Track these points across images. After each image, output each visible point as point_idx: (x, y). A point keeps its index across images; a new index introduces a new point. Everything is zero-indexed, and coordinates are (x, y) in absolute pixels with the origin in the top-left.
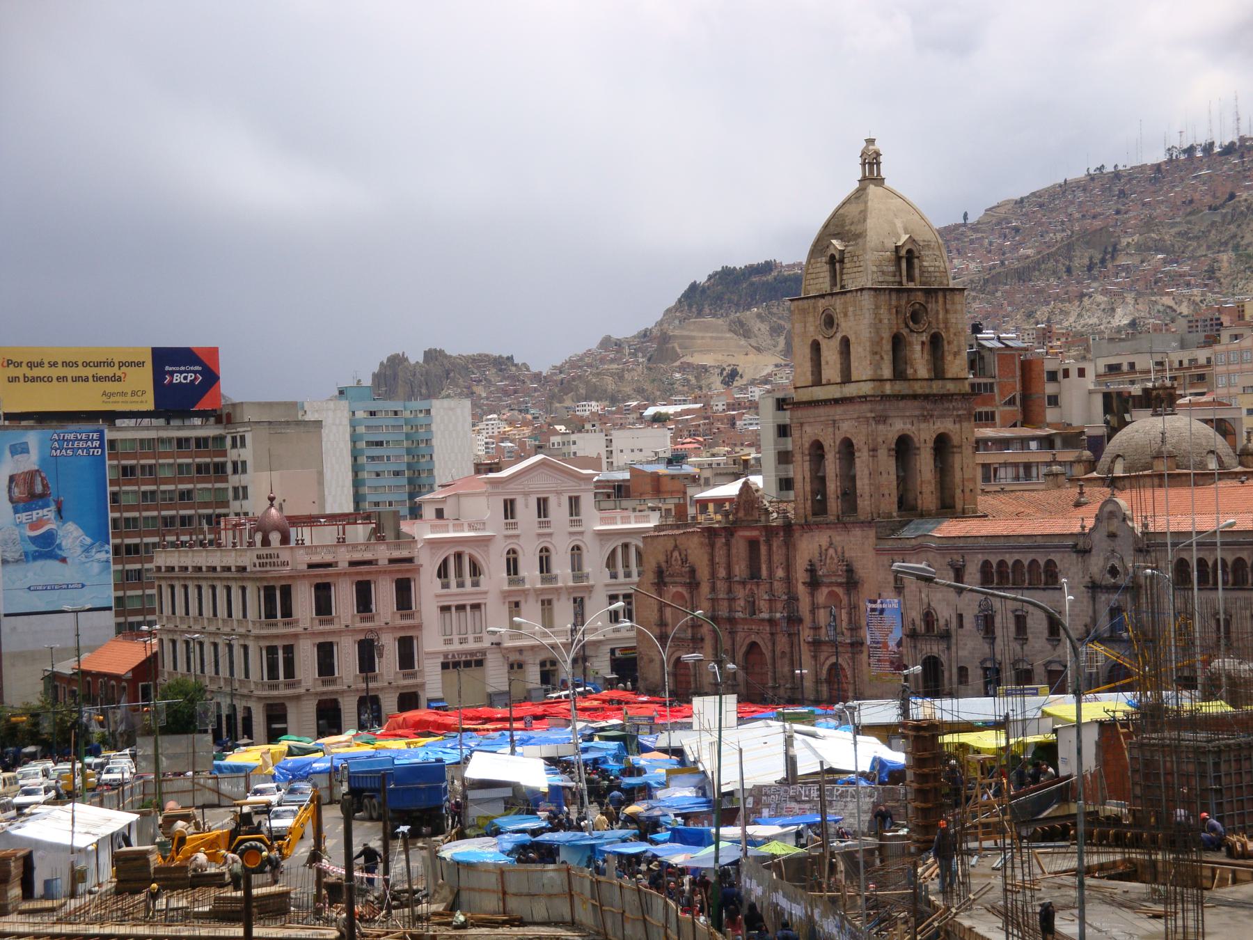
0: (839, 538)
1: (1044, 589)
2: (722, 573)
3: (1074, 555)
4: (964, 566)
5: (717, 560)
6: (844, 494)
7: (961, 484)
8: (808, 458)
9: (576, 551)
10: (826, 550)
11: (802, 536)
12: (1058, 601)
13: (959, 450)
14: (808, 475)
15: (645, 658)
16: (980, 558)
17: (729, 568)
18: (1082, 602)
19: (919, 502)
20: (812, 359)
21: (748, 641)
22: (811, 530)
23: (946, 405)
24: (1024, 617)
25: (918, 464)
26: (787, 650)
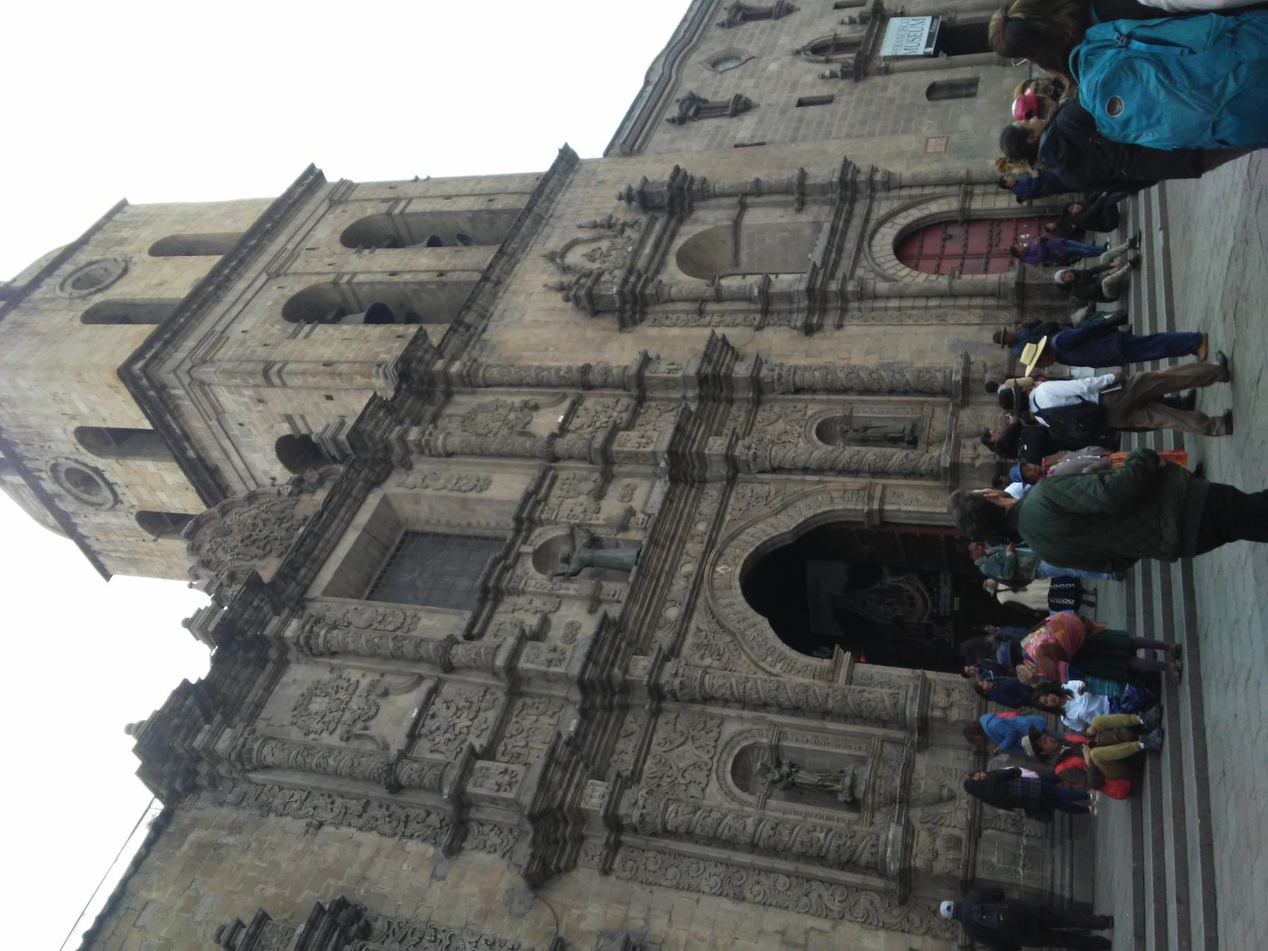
10: (566, 269)
21: (735, 603)
26: (816, 408)
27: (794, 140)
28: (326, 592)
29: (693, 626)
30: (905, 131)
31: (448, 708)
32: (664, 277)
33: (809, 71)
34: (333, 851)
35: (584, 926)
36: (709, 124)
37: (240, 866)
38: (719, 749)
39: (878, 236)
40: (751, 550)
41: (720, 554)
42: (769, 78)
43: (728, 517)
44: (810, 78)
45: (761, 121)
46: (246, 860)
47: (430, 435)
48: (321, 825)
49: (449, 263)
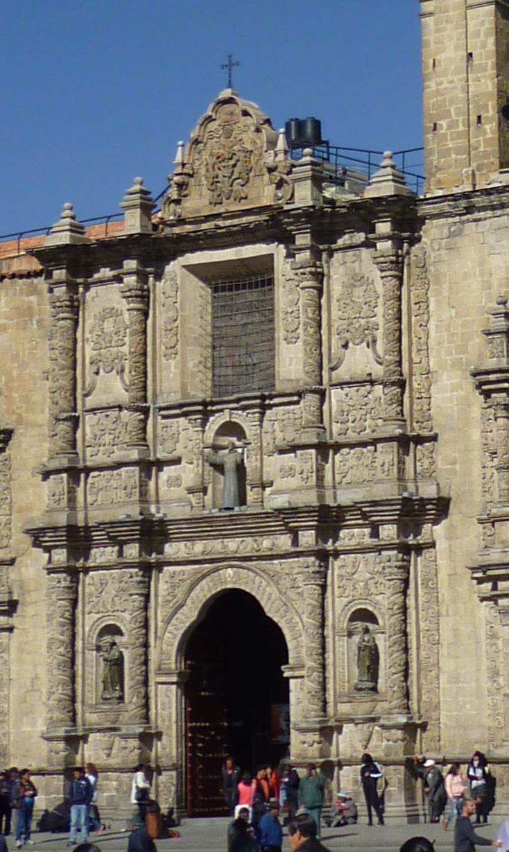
2: (113, 388)
5: (89, 353)
21: (206, 591)
28: (186, 267)
29: (189, 567)
31: (114, 422)
34: (37, 397)
35: (23, 569)
37: (23, 343)
38: (115, 614)
40: (248, 590)
41: (242, 568)
43: (276, 562)
46: (27, 345)
47: (304, 274)
48: (48, 379)
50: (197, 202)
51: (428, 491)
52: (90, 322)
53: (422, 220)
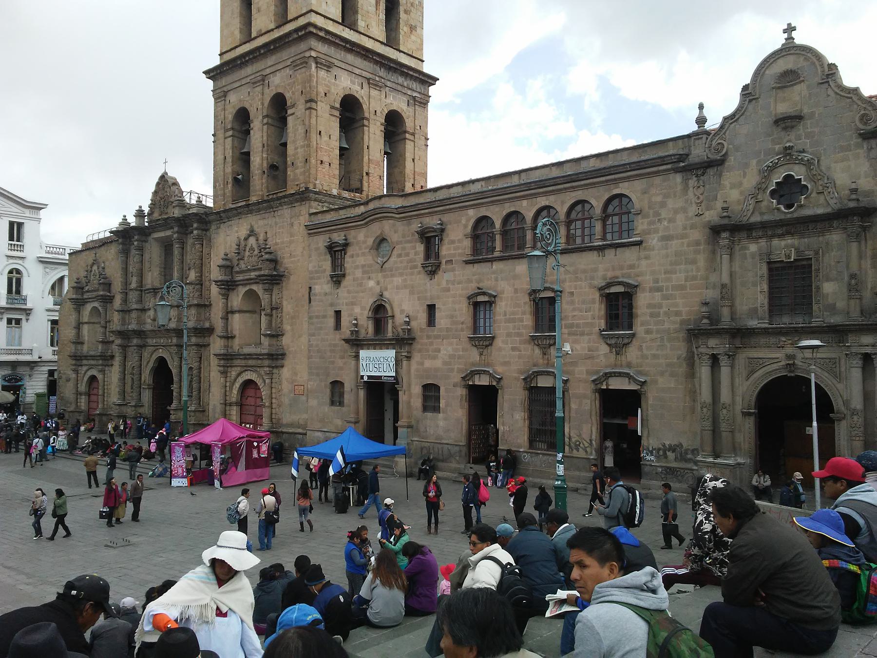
0: (259, 222)
1: (601, 249)
3: (678, 178)
4: (443, 230)
5: (131, 269)
6: (273, 167)
7: (412, 176)
8: (230, 133)
9: (14, 274)
11: (218, 228)
12: (632, 267)
13: (411, 137)
14: (229, 153)
15: (64, 377)
16: (472, 215)
17: (141, 275)
18: (694, 262)
19: (365, 184)
20: (241, 14)
21: (154, 357)
22: (229, 219)
23: (401, 80)
24: (552, 301)
25: (366, 137)
26: (195, 365)
27: (310, 318)
30: (310, 374)
32: (240, 288)
33: (363, 308)
36: (327, 265)
39: (252, 373)
42: (361, 285)
44: (357, 310)
45: (326, 294)
49: (256, 175)
50: (156, 215)
51: (207, 325)
52: (131, 258)
53: (210, 222)
